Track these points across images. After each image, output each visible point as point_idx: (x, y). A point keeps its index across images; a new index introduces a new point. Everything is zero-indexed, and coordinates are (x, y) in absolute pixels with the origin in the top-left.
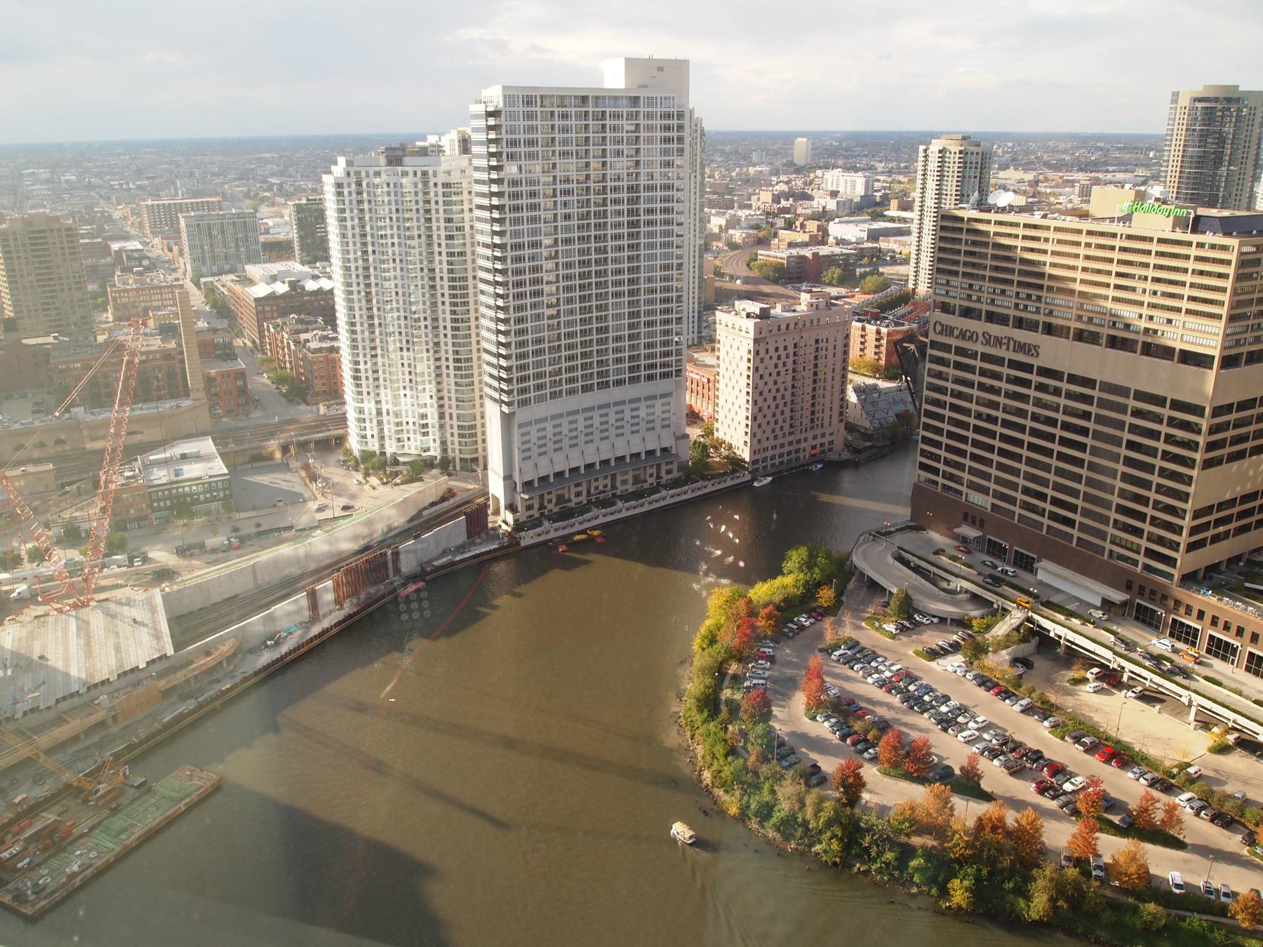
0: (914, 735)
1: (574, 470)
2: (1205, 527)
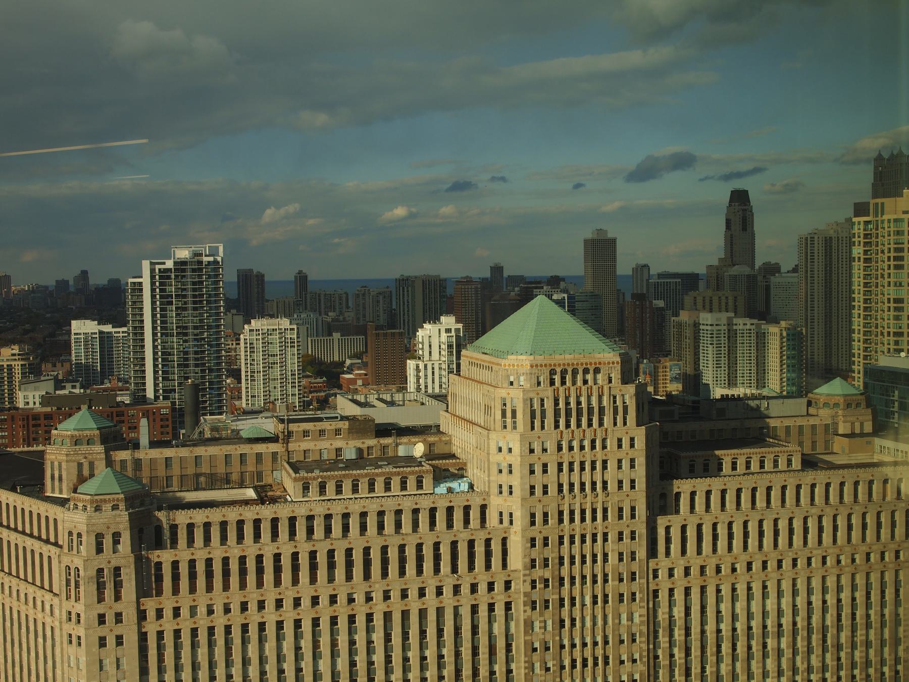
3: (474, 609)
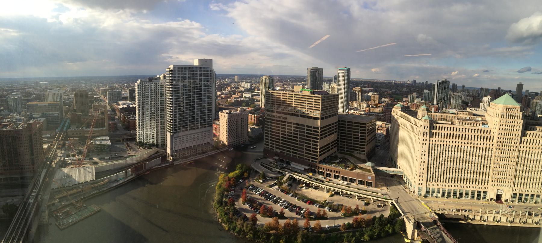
0: (269, 206)
2: (322, 151)
3: (486, 148)
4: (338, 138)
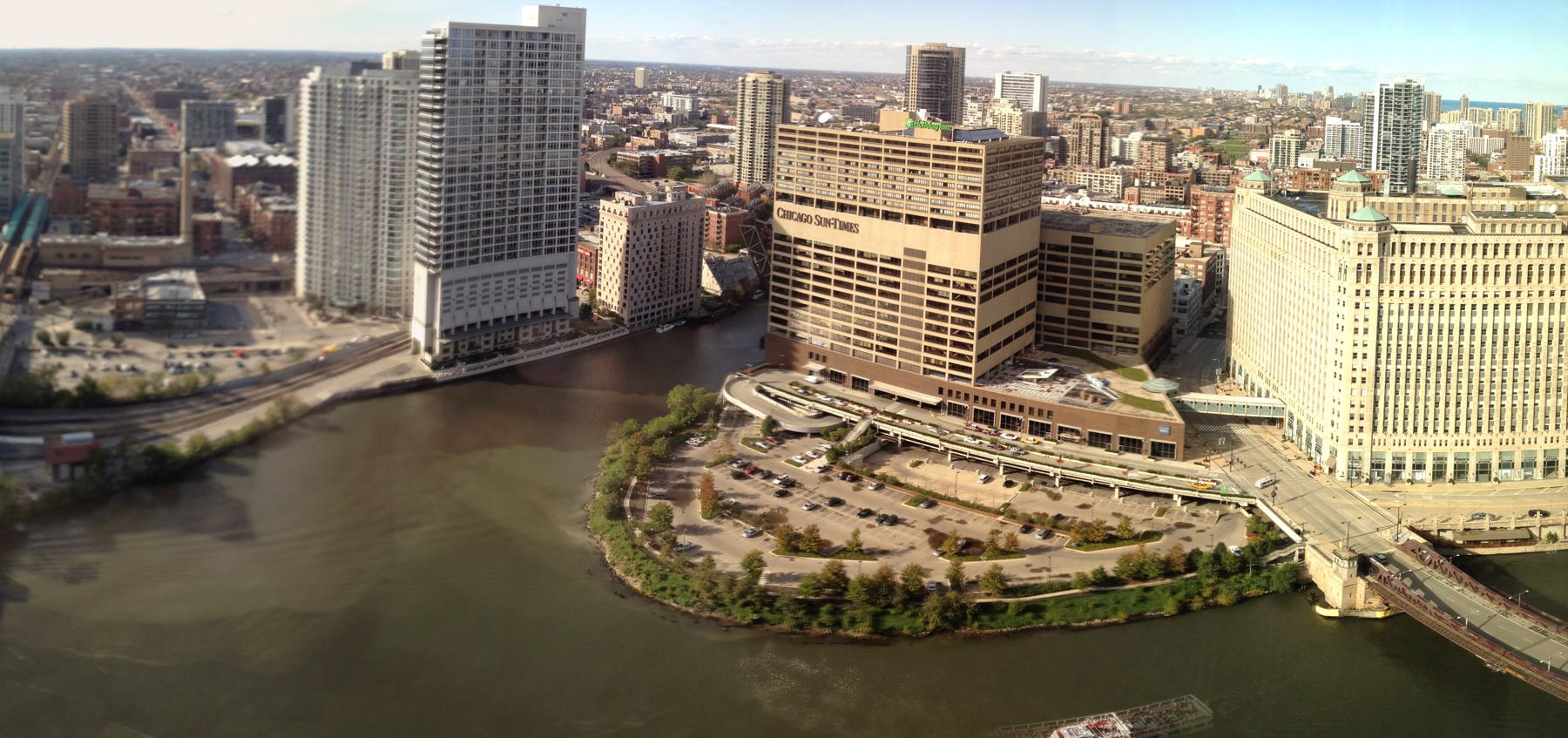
1: (485, 323)
4: (1039, 297)
